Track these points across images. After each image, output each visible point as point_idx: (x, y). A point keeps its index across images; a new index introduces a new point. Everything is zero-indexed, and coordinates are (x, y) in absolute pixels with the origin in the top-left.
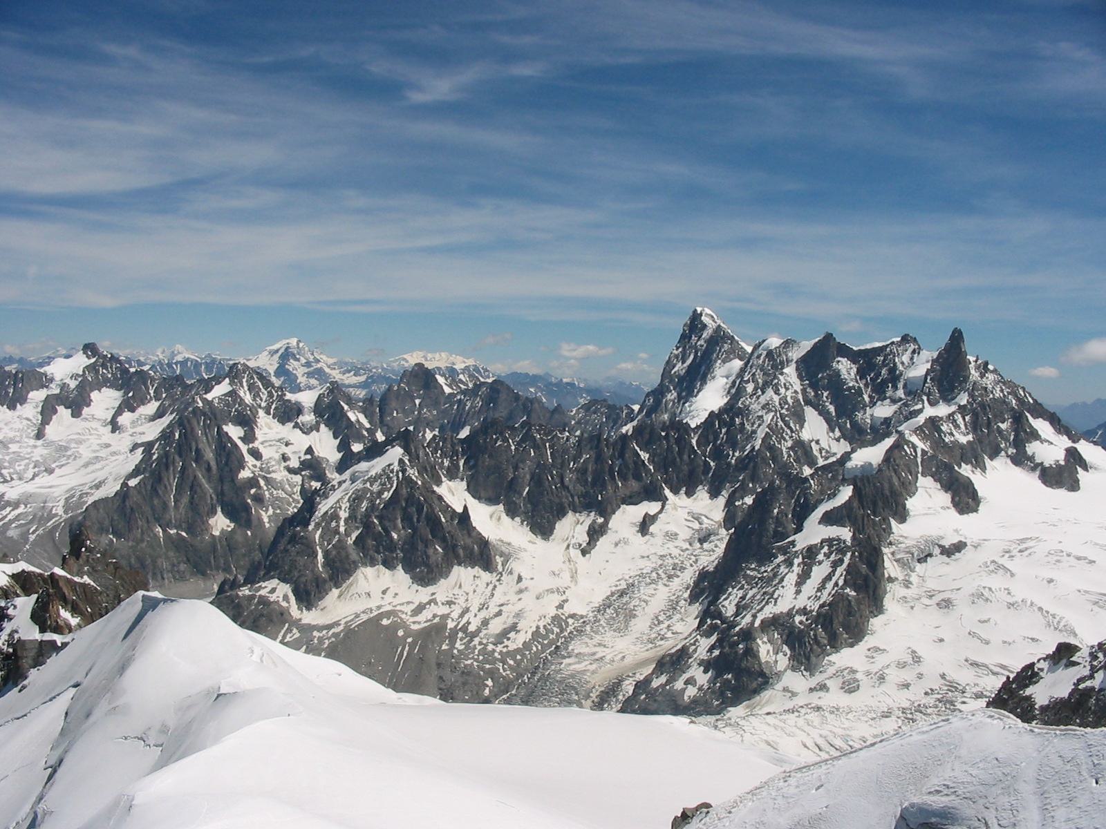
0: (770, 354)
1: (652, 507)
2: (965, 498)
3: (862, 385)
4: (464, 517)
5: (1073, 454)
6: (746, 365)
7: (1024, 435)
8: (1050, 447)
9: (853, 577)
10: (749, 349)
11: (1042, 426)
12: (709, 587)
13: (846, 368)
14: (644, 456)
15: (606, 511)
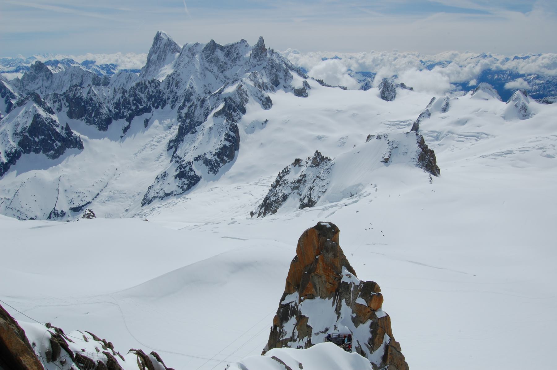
0: (190, 49)
1: (146, 115)
2: (267, 103)
3: (227, 61)
4: (68, 129)
5: (306, 84)
6: (181, 54)
7: (287, 77)
8: (298, 82)
9: (228, 138)
10: (182, 47)
11: (294, 74)
12: (174, 145)
13: (219, 54)
14: (142, 95)
15: (130, 119)
